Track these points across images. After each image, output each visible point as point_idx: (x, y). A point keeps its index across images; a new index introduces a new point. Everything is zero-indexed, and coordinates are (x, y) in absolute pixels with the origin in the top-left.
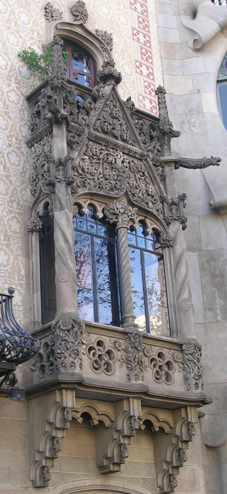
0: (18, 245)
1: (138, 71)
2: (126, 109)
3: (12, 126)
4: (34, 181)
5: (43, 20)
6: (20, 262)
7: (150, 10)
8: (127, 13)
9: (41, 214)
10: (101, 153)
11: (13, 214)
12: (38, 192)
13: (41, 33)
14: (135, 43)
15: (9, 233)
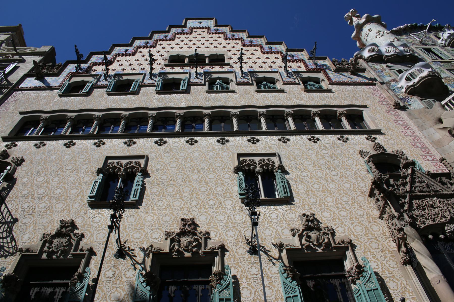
0: (399, 274)
1: (426, 160)
2: (426, 176)
3: (367, 212)
4: (392, 235)
5: (361, 158)
6: (405, 284)
7: (416, 132)
8: (404, 138)
9: (405, 251)
10: (423, 203)
11: (388, 258)
12: (397, 239)
13: (362, 164)
14: (417, 149)
15: (391, 269)
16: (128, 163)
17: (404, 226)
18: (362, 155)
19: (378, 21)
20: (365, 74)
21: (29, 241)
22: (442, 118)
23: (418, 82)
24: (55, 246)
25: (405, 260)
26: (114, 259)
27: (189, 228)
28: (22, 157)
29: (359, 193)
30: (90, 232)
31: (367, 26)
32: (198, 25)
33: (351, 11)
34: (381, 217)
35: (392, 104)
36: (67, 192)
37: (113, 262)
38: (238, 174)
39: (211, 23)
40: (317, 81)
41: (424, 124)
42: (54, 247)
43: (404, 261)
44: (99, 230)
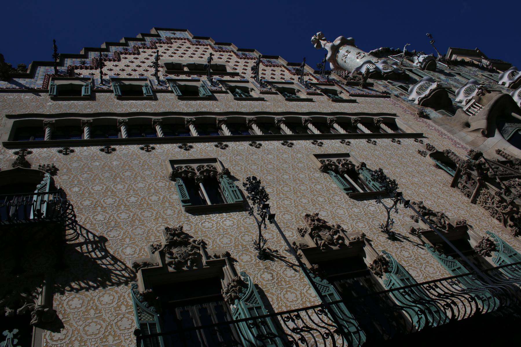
5: (423, 157)
16: (199, 166)
17: (514, 200)
18: (421, 154)
19: (351, 43)
20: (375, 88)
21: (136, 255)
22: (470, 121)
23: (429, 94)
24: (180, 256)
25: (516, 231)
26: (261, 261)
27: (320, 222)
28: (53, 164)
29: (442, 184)
30: (210, 238)
31: (344, 48)
32: (172, 36)
33: (318, 34)
34: (474, 202)
35: (416, 113)
36: (145, 200)
37: (261, 264)
38: (328, 173)
39: (187, 34)
40: (334, 92)
41: (452, 129)
42: (179, 258)
43: (515, 233)
44: (220, 235)
